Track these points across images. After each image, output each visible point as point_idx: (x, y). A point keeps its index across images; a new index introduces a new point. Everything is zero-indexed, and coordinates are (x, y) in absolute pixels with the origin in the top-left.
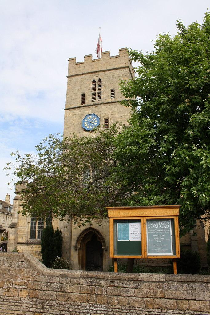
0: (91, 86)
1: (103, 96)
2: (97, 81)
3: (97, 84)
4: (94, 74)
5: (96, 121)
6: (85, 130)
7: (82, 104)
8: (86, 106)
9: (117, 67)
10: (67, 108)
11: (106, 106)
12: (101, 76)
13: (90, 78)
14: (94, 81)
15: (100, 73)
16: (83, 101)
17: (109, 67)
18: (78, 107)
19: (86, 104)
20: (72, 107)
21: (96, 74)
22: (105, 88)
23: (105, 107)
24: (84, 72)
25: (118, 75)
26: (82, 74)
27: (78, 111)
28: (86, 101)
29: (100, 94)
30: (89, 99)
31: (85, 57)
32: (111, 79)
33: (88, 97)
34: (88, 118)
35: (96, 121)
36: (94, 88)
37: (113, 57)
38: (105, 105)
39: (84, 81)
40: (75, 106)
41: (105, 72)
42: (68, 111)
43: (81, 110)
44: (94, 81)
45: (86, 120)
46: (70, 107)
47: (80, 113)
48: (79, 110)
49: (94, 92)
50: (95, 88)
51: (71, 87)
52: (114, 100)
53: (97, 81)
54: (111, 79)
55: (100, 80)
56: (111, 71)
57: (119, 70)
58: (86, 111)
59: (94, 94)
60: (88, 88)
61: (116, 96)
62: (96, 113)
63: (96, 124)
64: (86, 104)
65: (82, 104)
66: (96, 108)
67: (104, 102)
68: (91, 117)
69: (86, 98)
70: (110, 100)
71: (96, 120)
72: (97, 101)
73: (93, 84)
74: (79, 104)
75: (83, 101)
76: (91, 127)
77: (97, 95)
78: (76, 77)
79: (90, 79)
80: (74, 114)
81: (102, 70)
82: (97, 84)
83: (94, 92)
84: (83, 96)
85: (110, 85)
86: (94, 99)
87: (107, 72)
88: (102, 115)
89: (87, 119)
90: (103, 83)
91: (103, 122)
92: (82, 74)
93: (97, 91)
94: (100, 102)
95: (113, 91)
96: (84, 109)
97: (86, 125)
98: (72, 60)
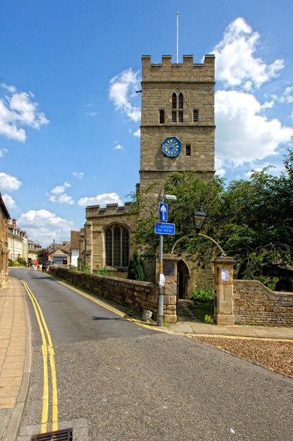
0: (171, 100)
1: (185, 116)
2: (177, 95)
3: (178, 100)
4: (174, 85)
5: (177, 147)
8: (166, 126)
9: (201, 80)
10: (146, 124)
14: (174, 95)
15: (181, 85)
17: (193, 79)
18: (156, 127)
19: (166, 123)
20: (149, 124)
28: (166, 120)
29: (181, 113)
31: (163, 58)
34: (168, 142)
35: (177, 147)
44: (174, 95)
50: (176, 104)
52: (197, 123)
53: (177, 95)
55: (181, 95)
59: (174, 113)
61: (200, 117)
64: (166, 123)
70: (193, 123)
72: (178, 123)
74: (157, 121)
75: (162, 120)
77: (177, 112)
82: (178, 100)
84: (162, 112)
86: (174, 120)
90: (185, 100)
95: (196, 112)
97: (166, 150)
98: (146, 59)
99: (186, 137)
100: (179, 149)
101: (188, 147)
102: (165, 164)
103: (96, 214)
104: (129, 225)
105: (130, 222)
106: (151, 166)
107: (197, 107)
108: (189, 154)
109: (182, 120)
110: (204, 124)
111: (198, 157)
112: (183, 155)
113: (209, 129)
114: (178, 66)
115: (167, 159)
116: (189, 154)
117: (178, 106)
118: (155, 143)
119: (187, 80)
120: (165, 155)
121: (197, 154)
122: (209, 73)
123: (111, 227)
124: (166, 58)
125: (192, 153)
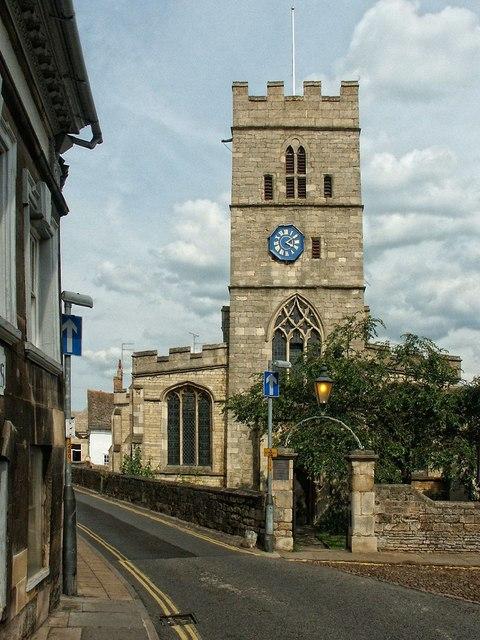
0: (284, 159)
1: (309, 188)
3: (297, 160)
4: (288, 132)
5: (297, 242)
6: (275, 258)
7: (266, 199)
8: (276, 206)
9: (336, 123)
11: (315, 212)
13: (281, 141)
14: (290, 149)
15: (301, 133)
16: (269, 193)
19: (276, 201)
22: (312, 170)
23: (314, 212)
27: (260, 216)
28: (276, 194)
29: (302, 182)
34: (281, 233)
36: (289, 168)
37: (329, 99)
40: (252, 202)
42: (239, 212)
44: (290, 149)
46: (244, 201)
47: (263, 219)
49: (289, 176)
55: (301, 149)
56: (326, 133)
57: (341, 132)
58: (280, 218)
59: (290, 181)
60: (279, 165)
62: (297, 225)
63: (296, 248)
65: (266, 199)
66: (296, 213)
68: (286, 232)
70: (323, 200)
71: (296, 239)
72: (296, 199)
73: (287, 157)
75: (269, 193)
76: (287, 254)
78: (250, 132)
81: (305, 124)
82: (297, 160)
83: (289, 176)
84: (268, 179)
86: (290, 194)
87: (317, 135)
88: (307, 230)
90: (309, 159)
91: (310, 247)
93: (296, 174)
94: (302, 201)
95: (328, 179)
96: (272, 212)
97: (277, 248)
98: (239, 87)
99: (313, 222)
100: (302, 245)
101: (316, 242)
102: (274, 273)
103: (153, 366)
104: (211, 388)
105: (212, 381)
106: (249, 276)
107: (329, 171)
108: (316, 254)
109: (303, 194)
110: (342, 201)
111: (335, 260)
112: (306, 257)
113: (352, 210)
114: (294, 99)
115: (277, 264)
116: (316, 254)
117: (296, 170)
118: (257, 236)
120: (275, 258)
121: (332, 255)
122: (349, 113)
123: (178, 390)
124: (276, 86)
125: (323, 255)
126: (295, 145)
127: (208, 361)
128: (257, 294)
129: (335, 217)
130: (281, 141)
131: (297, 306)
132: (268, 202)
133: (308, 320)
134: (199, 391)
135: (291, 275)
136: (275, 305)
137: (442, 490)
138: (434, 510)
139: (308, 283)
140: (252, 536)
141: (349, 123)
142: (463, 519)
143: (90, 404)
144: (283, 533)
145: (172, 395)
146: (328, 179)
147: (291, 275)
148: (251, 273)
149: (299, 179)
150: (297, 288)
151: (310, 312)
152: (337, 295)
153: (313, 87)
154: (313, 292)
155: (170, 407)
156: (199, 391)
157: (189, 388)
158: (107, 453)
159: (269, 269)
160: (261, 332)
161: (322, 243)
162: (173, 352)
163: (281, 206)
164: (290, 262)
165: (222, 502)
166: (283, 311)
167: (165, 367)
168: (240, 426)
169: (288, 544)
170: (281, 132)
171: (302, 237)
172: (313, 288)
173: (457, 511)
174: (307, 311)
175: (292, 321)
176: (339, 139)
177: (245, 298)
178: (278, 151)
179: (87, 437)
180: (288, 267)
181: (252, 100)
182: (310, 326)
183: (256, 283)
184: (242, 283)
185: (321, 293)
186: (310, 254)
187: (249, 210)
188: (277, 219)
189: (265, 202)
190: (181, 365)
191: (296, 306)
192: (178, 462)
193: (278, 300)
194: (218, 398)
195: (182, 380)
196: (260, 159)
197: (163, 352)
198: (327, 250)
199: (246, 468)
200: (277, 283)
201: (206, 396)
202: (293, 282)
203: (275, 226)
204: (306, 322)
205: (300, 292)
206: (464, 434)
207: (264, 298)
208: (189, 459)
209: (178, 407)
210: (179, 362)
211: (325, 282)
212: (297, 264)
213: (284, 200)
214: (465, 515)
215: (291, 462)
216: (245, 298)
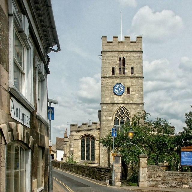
0: (118, 62)
1: (126, 71)
3: (122, 62)
4: (120, 53)
5: (122, 89)
6: (115, 94)
7: (112, 75)
9: (135, 50)
10: (103, 76)
11: (129, 79)
12: (125, 55)
13: (118, 56)
14: (120, 58)
15: (124, 53)
16: (113, 73)
17: (130, 50)
19: (116, 75)
21: (121, 53)
23: (128, 79)
24: (113, 50)
25: (136, 57)
26: (112, 51)
27: (110, 80)
28: (115, 73)
29: (124, 69)
30: (117, 71)
32: (131, 59)
33: (116, 70)
34: (117, 86)
36: (120, 65)
38: (127, 78)
39: (113, 57)
41: (127, 53)
42: (104, 79)
43: (113, 79)
44: (120, 58)
45: (116, 87)
46: (106, 75)
48: (110, 79)
49: (120, 67)
51: (104, 60)
52: (133, 75)
54: (131, 59)
55: (124, 58)
58: (117, 81)
59: (120, 69)
61: (134, 72)
62: (122, 83)
63: (122, 91)
65: (112, 75)
67: (127, 76)
68: (119, 85)
69: (115, 71)
70: (130, 75)
72: (122, 75)
73: (119, 61)
74: (110, 74)
75: (113, 73)
76: (119, 93)
78: (107, 53)
79: (118, 57)
80: (108, 81)
82: (122, 62)
84: (113, 68)
85: (131, 63)
86: (120, 73)
87: (129, 53)
89: (117, 87)
90: (126, 62)
92: (112, 51)
93: (122, 67)
94: (124, 75)
95: (132, 68)
96: (114, 79)
97: (116, 91)
98: (104, 38)
99: (128, 82)
100: (124, 90)
101: (128, 89)
102: (115, 99)
104: (95, 136)
105: (95, 134)
106: (108, 100)
107: (133, 66)
108: (128, 93)
109: (124, 73)
110: (137, 75)
111: (135, 94)
112: (125, 94)
113: (140, 78)
114: (121, 42)
115: (116, 96)
116: (128, 93)
117: (122, 65)
118: (110, 87)
119: (127, 50)
120: (115, 94)
121: (133, 93)
122: (139, 46)
123: (84, 136)
124: (115, 37)
125: (130, 93)
126: (122, 57)
127: (94, 127)
128: (110, 106)
129: (134, 81)
130: (118, 56)
131: (122, 110)
132: (113, 76)
133: (126, 114)
134: (91, 137)
135: (120, 100)
136: (115, 109)
137: (169, 168)
138: (166, 174)
139: (126, 102)
140: (108, 181)
141: (139, 50)
142: (175, 177)
143: (57, 141)
144: (118, 180)
145: (83, 138)
146: (132, 68)
147: (120, 100)
148: (108, 99)
149: (123, 68)
150: (122, 104)
151: (126, 112)
152: (135, 106)
153: (127, 37)
154: (127, 105)
155: (82, 142)
156: (91, 137)
157: (88, 136)
158: (62, 157)
159: (113, 98)
160: (111, 118)
161: (130, 89)
162: (83, 124)
163: (117, 77)
164: (120, 95)
165: (98, 171)
166: (118, 111)
167: (81, 129)
168: (105, 148)
169: (119, 183)
170: (117, 53)
171: (124, 87)
172: (127, 104)
173: (173, 174)
174: (125, 111)
175: (121, 115)
176: (136, 55)
177: (106, 107)
178: (116, 59)
179: (56, 152)
180: (119, 97)
181: (108, 42)
182: (126, 116)
183: (109, 102)
184: (105, 102)
185: (130, 105)
186: (126, 93)
187: (107, 78)
188: (116, 81)
189: (112, 76)
190: (85, 129)
191: (122, 110)
192: (85, 160)
193: (116, 108)
194: (97, 139)
195: (86, 133)
196: (111, 62)
197: (80, 125)
198: (132, 91)
199: (106, 161)
200: (116, 102)
201: (93, 138)
202: (121, 102)
203: (115, 83)
204: (125, 115)
205: (123, 105)
206: (176, 151)
207: (112, 107)
208: (88, 159)
209: (84, 142)
210: (85, 128)
211: (131, 102)
212: (122, 96)
213: (118, 75)
214: (176, 176)
215: (120, 158)
216: (106, 107)
